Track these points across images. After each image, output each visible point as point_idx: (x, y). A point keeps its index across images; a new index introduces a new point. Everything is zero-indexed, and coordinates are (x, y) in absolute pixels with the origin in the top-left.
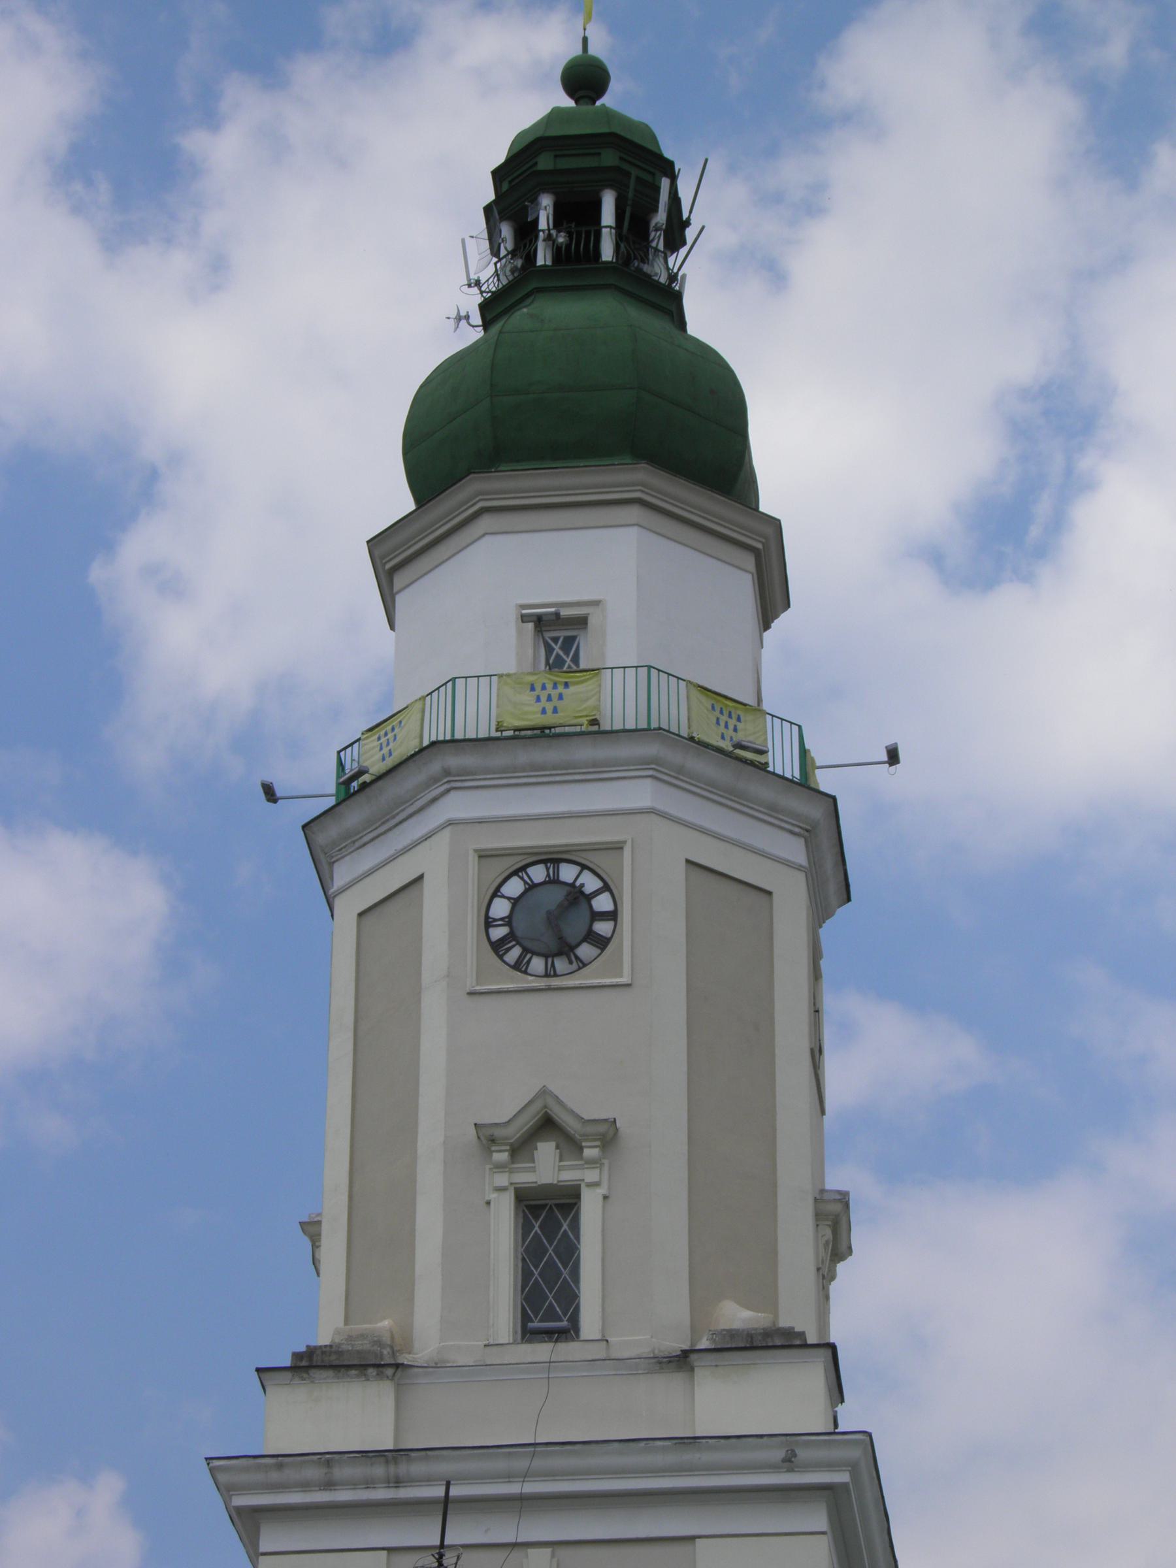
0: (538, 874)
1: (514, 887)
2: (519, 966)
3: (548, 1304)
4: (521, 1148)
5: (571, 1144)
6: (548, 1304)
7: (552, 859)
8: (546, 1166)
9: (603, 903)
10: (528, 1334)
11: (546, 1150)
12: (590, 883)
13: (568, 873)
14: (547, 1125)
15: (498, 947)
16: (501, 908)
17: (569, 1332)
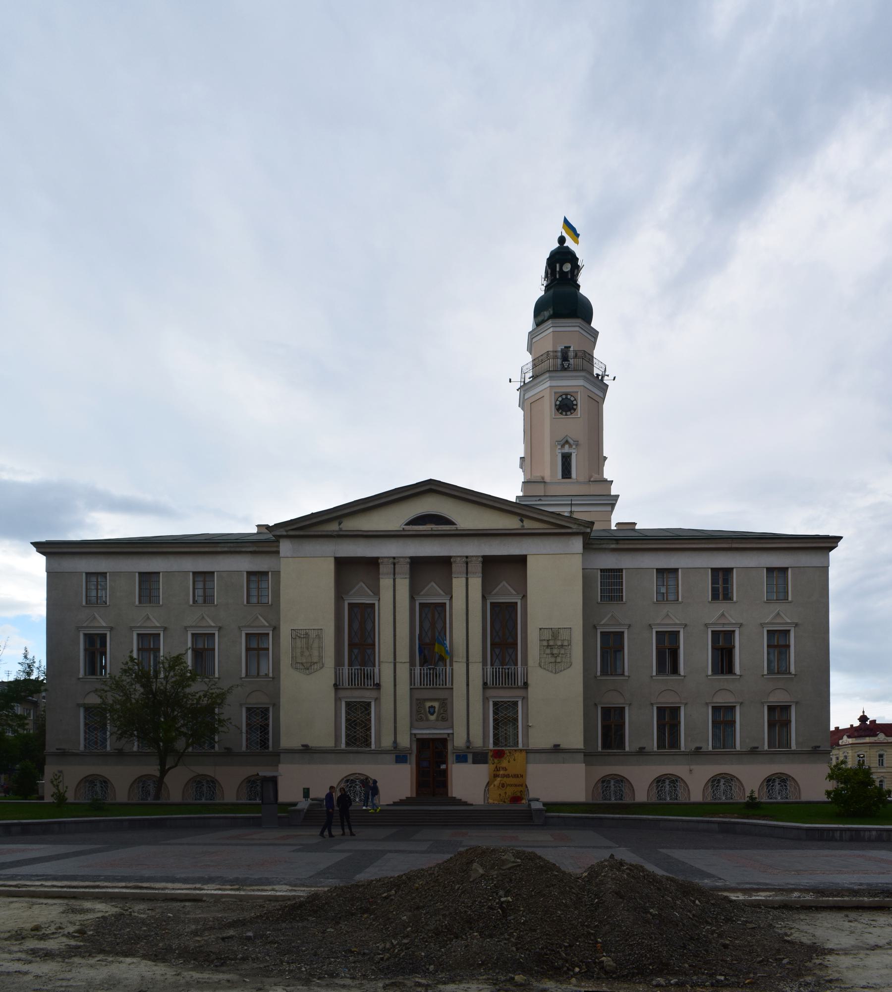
0: (564, 397)
1: (560, 399)
2: (561, 413)
3: (566, 472)
4: (563, 446)
5: (570, 446)
6: (566, 472)
7: (566, 395)
8: (566, 449)
9: (575, 402)
10: (563, 477)
11: (567, 446)
12: (572, 399)
13: (569, 397)
14: (567, 442)
15: (558, 410)
16: (558, 403)
17: (570, 478)
